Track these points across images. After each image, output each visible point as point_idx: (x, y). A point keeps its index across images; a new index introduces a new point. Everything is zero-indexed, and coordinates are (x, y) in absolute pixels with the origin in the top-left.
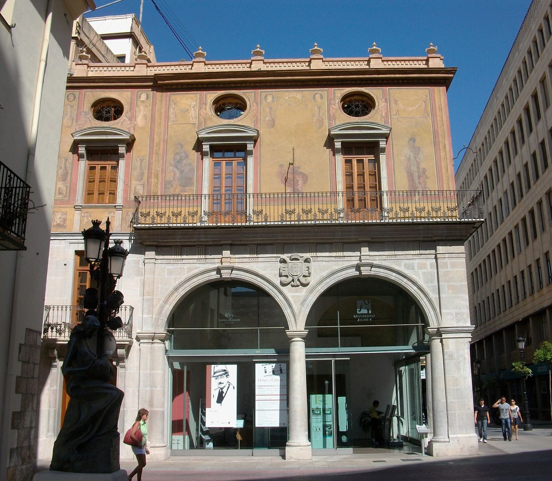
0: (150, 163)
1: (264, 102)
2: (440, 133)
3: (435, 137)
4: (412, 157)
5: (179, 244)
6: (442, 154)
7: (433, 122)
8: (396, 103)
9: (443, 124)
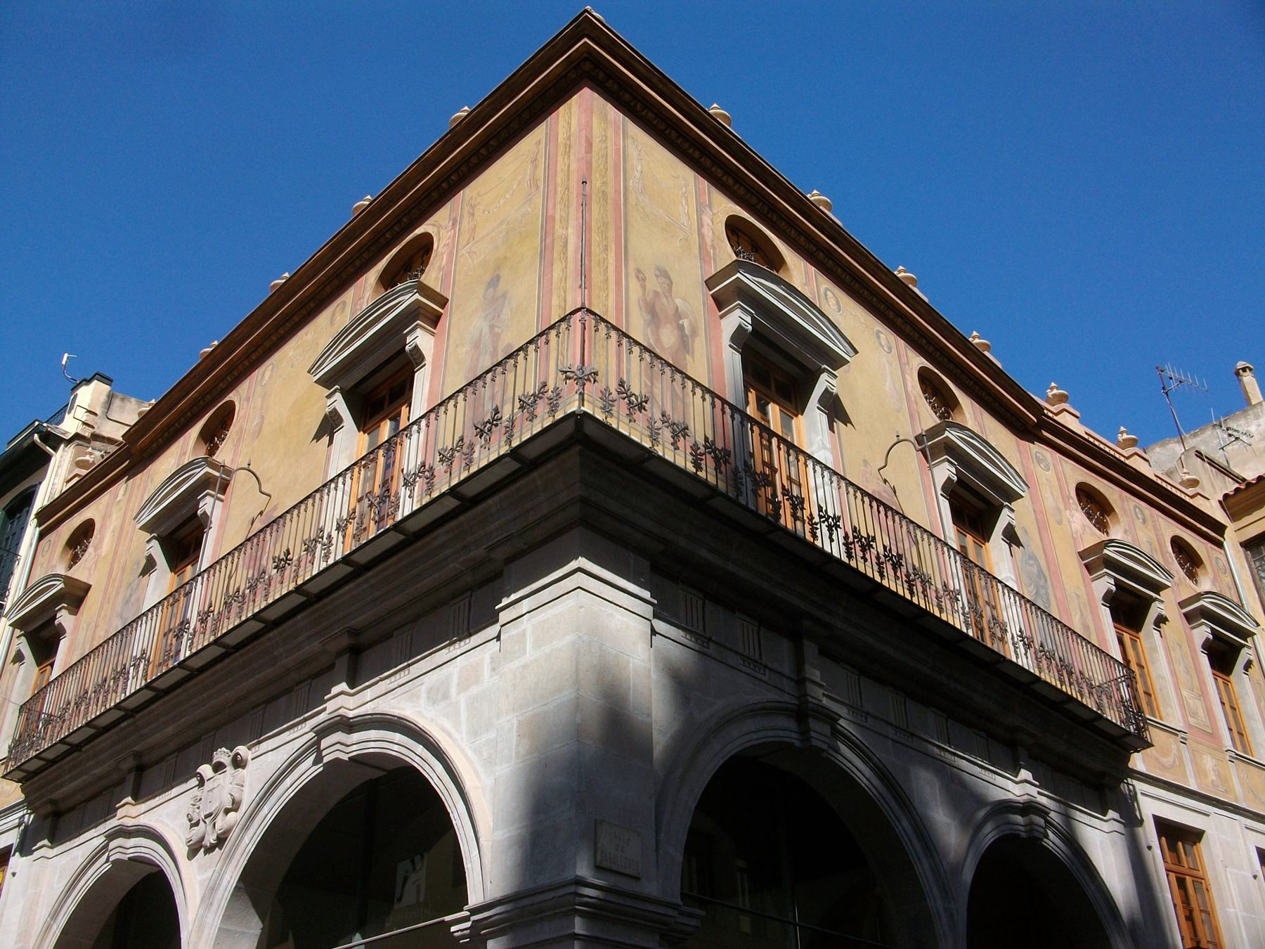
0: (96, 626)
1: (259, 389)
2: (557, 217)
3: (543, 239)
4: (486, 329)
5: (79, 797)
6: (557, 274)
7: (546, 199)
8: (473, 214)
9: (568, 188)
